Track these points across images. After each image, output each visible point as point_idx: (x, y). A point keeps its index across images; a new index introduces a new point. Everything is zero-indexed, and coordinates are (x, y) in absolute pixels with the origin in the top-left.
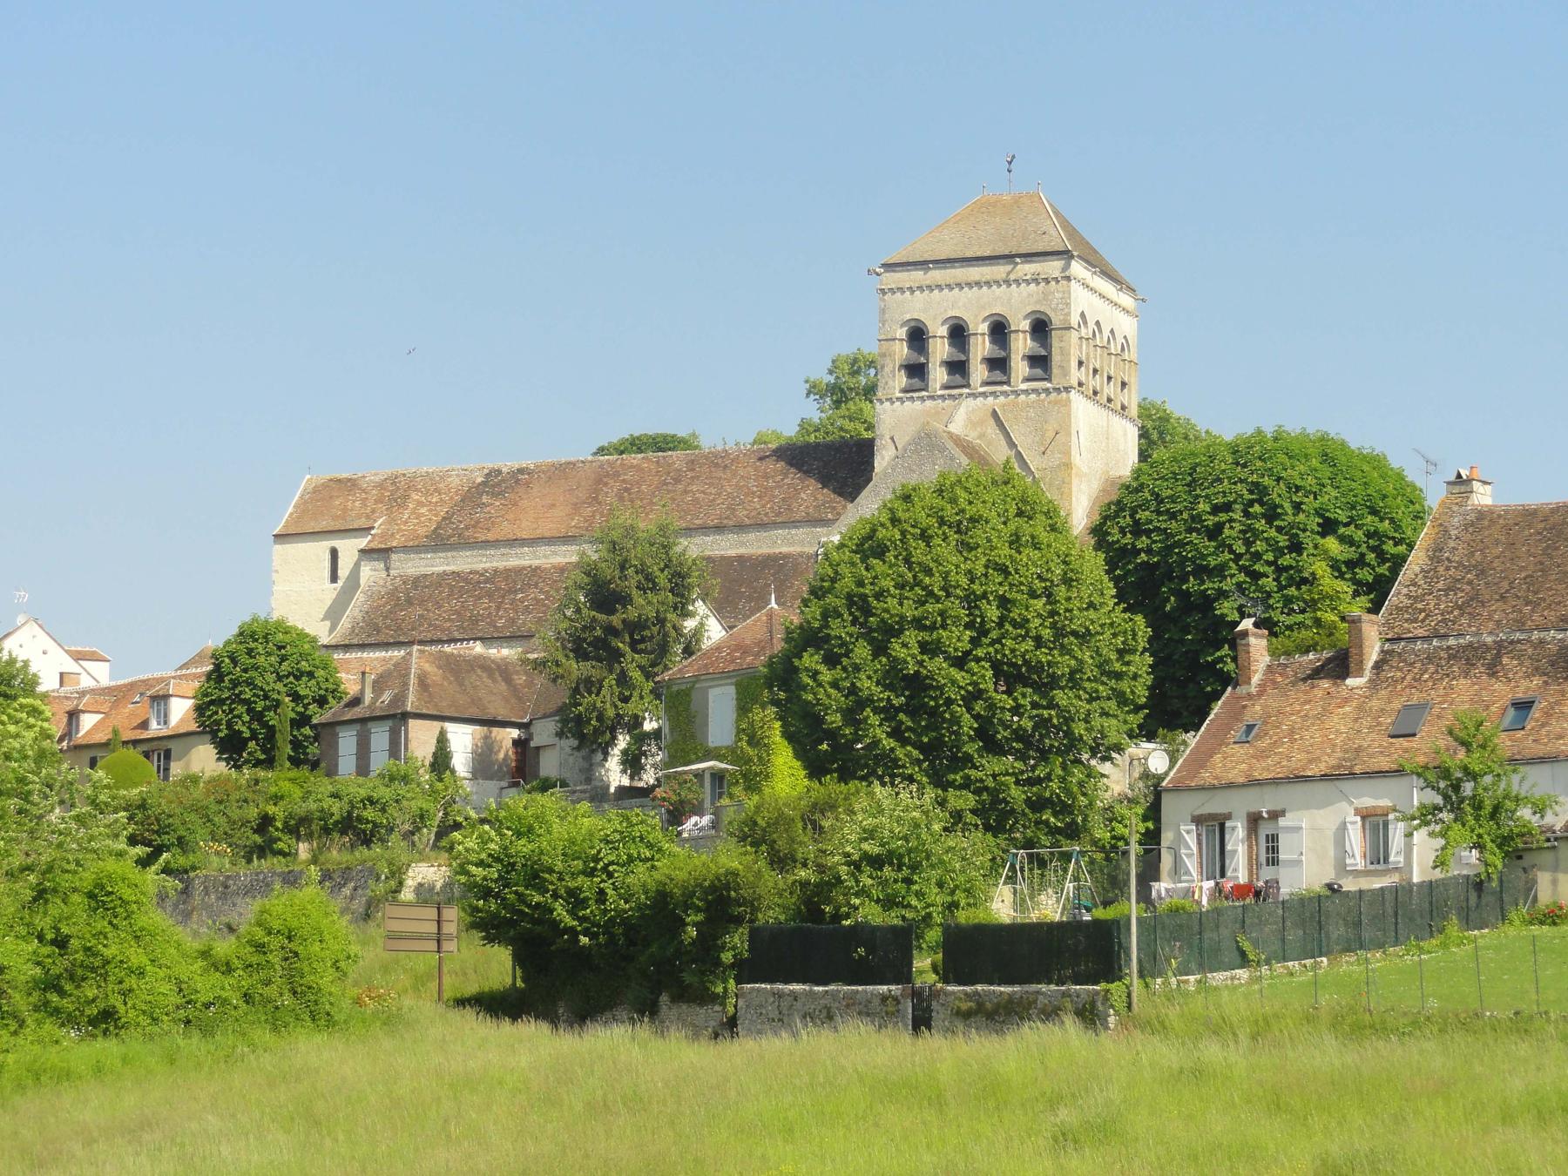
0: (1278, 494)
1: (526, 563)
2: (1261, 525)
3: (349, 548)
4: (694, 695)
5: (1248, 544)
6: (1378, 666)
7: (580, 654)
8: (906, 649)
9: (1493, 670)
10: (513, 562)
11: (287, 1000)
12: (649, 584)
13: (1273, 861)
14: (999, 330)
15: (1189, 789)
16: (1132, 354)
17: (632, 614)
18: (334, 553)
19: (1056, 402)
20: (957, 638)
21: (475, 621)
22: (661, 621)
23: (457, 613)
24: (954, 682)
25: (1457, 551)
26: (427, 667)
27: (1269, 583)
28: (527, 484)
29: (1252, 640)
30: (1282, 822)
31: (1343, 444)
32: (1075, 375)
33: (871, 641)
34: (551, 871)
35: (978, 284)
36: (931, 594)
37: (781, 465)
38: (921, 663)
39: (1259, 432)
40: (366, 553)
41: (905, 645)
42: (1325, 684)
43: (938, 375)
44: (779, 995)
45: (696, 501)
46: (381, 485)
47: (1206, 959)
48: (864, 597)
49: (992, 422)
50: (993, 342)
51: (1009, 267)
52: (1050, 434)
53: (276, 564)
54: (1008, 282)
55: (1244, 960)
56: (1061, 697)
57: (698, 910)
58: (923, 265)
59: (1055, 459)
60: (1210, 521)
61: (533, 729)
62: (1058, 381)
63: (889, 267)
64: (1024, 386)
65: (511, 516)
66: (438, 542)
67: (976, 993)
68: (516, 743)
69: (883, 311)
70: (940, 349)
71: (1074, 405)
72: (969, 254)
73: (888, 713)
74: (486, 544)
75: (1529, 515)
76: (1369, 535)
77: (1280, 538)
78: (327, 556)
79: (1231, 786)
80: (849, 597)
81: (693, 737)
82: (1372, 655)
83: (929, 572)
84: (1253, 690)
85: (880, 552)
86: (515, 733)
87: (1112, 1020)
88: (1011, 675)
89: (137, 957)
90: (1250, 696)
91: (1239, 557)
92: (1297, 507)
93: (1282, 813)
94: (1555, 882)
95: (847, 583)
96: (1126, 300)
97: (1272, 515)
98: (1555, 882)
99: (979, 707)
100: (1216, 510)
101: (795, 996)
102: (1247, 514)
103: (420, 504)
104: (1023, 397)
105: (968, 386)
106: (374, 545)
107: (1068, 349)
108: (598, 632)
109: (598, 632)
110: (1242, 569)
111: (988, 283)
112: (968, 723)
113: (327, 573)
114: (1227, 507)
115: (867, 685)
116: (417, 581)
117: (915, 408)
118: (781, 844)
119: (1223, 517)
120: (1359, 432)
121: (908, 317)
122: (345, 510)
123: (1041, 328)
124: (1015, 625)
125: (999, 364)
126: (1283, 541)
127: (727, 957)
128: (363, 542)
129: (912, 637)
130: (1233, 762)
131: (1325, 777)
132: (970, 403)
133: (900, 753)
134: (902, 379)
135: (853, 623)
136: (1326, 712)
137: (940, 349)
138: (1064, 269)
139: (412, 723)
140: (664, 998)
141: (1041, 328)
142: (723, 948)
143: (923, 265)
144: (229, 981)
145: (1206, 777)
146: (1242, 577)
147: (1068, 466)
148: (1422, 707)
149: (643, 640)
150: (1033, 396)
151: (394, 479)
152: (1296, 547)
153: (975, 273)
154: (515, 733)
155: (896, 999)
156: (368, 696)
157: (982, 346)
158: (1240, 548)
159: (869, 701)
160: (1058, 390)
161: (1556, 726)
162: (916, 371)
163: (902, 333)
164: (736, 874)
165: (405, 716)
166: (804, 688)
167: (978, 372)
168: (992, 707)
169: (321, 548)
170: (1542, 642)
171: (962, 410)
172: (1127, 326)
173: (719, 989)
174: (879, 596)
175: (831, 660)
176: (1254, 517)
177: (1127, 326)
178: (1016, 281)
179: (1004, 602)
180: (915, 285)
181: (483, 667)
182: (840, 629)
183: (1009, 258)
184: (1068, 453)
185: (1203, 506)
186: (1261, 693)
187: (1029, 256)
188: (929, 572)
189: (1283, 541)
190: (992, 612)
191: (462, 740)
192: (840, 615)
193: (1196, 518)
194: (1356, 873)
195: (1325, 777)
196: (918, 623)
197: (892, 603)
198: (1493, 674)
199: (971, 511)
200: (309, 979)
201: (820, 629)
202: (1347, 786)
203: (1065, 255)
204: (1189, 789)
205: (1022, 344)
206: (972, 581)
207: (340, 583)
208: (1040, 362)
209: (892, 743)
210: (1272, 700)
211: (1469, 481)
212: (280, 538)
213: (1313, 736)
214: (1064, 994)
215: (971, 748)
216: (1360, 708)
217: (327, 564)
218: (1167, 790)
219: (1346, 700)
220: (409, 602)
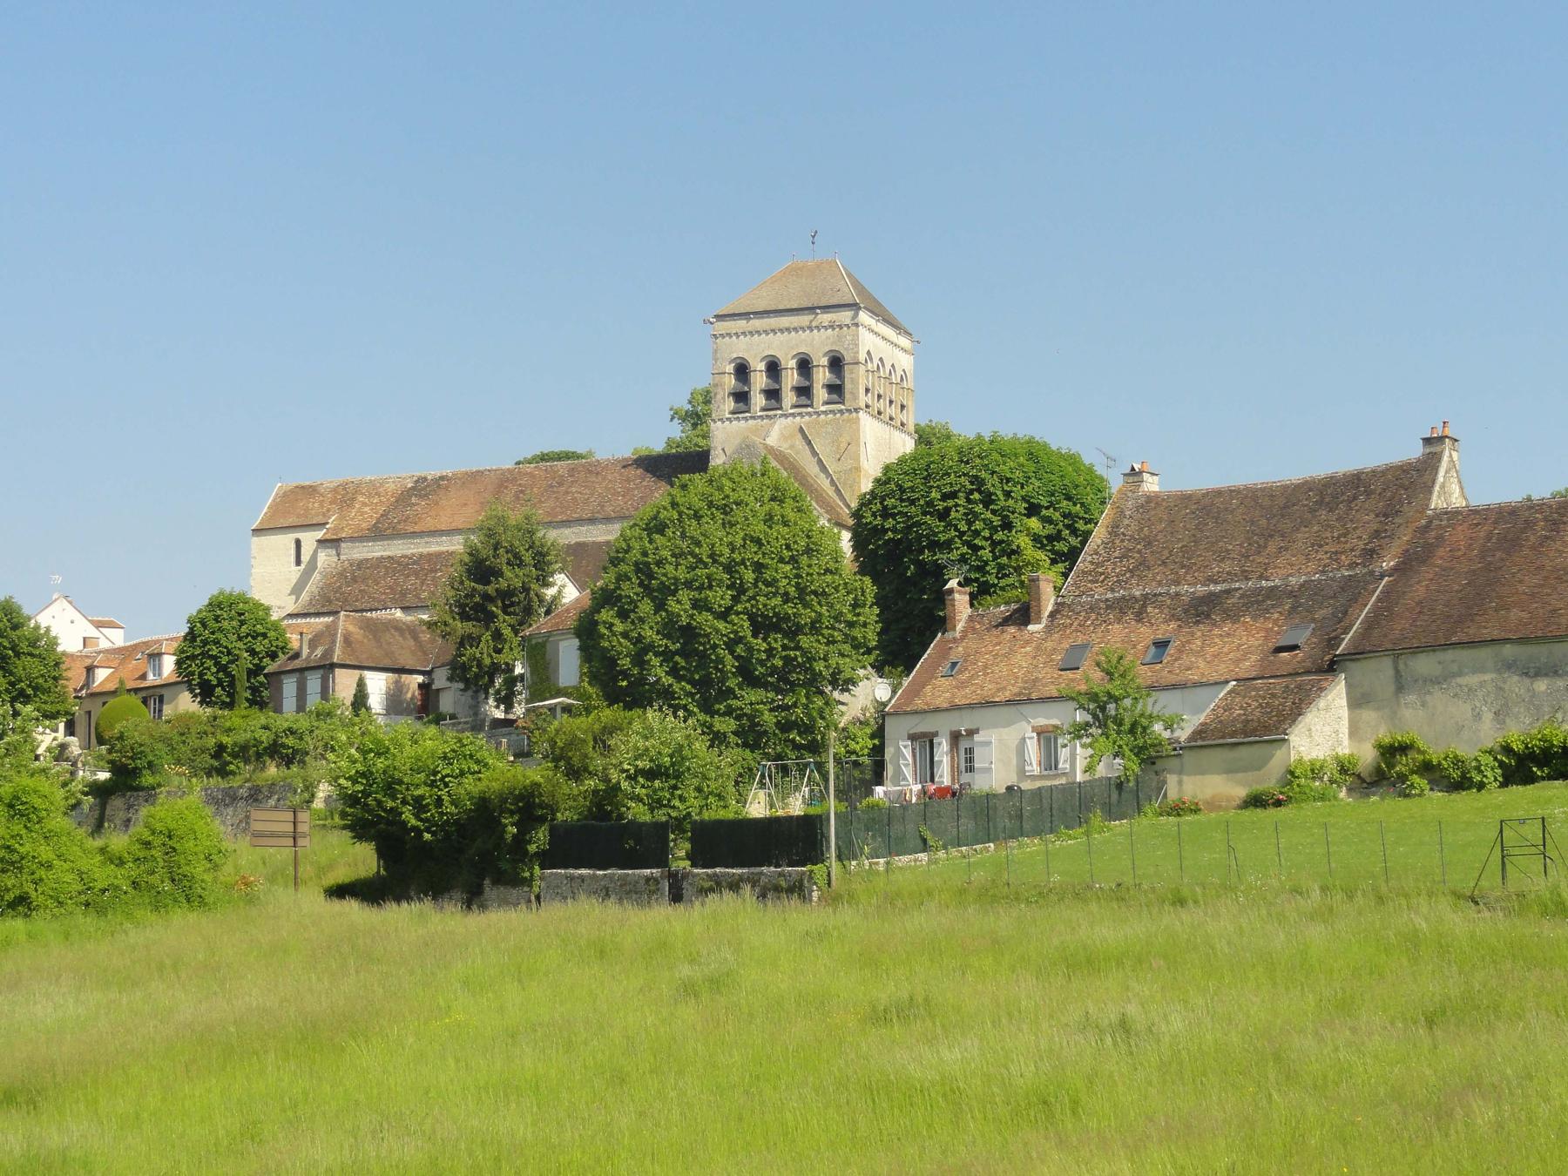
0: (992, 484)
1: (443, 549)
2: (979, 508)
3: (309, 539)
4: (548, 646)
5: (970, 523)
6: (1052, 615)
7: (464, 617)
8: (680, 605)
9: (1140, 617)
10: (434, 549)
11: (167, 886)
12: (516, 561)
13: (970, 769)
14: (805, 365)
15: (906, 713)
16: (911, 385)
17: (503, 584)
18: (298, 543)
20: (720, 597)
21: (403, 594)
22: (526, 589)
23: (391, 588)
24: (717, 631)
25: (1130, 526)
26: (351, 628)
27: (986, 554)
28: (447, 488)
29: (957, 596)
30: (977, 738)
31: (1045, 444)
32: (863, 399)
33: (653, 599)
34: (400, 782)
35: (788, 330)
36: (701, 561)
37: (639, 471)
38: (692, 616)
39: (979, 436)
40: (319, 541)
41: (679, 602)
42: (1012, 630)
43: (758, 400)
44: (572, 878)
45: (574, 499)
46: (335, 490)
47: (894, 846)
48: (647, 564)
49: (799, 436)
50: (800, 374)
52: (844, 445)
53: (254, 552)
54: (810, 328)
55: (925, 846)
56: (805, 641)
57: (512, 813)
58: (745, 315)
59: (847, 464)
60: (941, 506)
61: (434, 676)
62: (849, 404)
63: (720, 317)
64: (823, 408)
65: (433, 513)
66: (377, 533)
67: (715, 874)
68: (421, 686)
69: (716, 351)
70: (759, 380)
71: (862, 422)
72: (781, 307)
73: (667, 656)
74: (414, 535)
75: (1185, 499)
76: (1065, 516)
77: (994, 518)
78: (293, 546)
79: (937, 710)
80: (636, 564)
81: (548, 678)
82: (1049, 607)
83: (698, 544)
84: (958, 635)
85: (661, 528)
86: (420, 679)
87: (815, 894)
88: (762, 625)
89: (45, 852)
90: (955, 640)
91: (962, 534)
92: (1008, 494)
93: (977, 731)
94: (1180, 783)
95: (635, 555)
96: (904, 342)
97: (988, 501)
98: (1180, 783)
99: (739, 650)
100: (945, 497)
101: (582, 878)
102: (969, 501)
103: (364, 504)
105: (780, 408)
106: (328, 536)
107: (858, 380)
108: (477, 599)
109: (477, 599)
110: (966, 543)
111: (795, 329)
112: (730, 663)
113: (293, 559)
114: (953, 495)
115: (649, 634)
116: (361, 564)
117: (739, 426)
118: (576, 761)
119: (950, 503)
120: (1058, 437)
122: (307, 510)
123: (836, 363)
124: (768, 584)
125: (804, 391)
126: (997, 521)
127: (532, 848)
128: (320, 534)
129: (685, 595)
130: (940, 691)
131: (1009, 703)
133: (676, 687)
134: (730, 404)
135: (640, 585)
136: (1012, 651)
137: (759, 380)
139: (338, 671)
140: (487, 882)
141: (836, 363)
142: (529, 842)
143: (745, 315)
144: (121, 872)
145: (919, 703)
146: (965, 549)
147: (858, 469)
148: (1084, 647)
149: (512, 604)
151: (344, 486)
152: (1007, 526)
153: (785, 321)
154: (420, 679)
155: (656, 881)
156: (305, 651)
157: (791, 378)
158: (963, 527)
159: (650, 647)
160: (849, 411)
161: (1186, 660)
162: (742, 397)
163: (730, 368)
164: (538, 785)
165: (332, 666)
166: (602, 636)
167: (789, 398)
168: (750, 649)
169: (287, 540)
170: (1177, 594)
172: (905, 362)
173: (527, 874)
174: (659, 563)
175: (623, 615)
176: (975, 502)
177: (905, 362)
179: (759, 567)
181: (397, 628)
182: (630, 590)
183: (811, 310)
184: (857, 459)
185: (935, 494)
186: (963, 638)
187: (827, 308)
188: (698, 544)
189: (997, 521)
190: (749, 576)
191: (377, 685)
192: (629, 579)
193: (930, 504)
194: (1033, 778)
195: (1009, 703)
196: (688, 584)
197: (670, 568)
198: (1139, 621)
199: (734, 497)
200: (185, 869)
201: (614, 591)
202: (1027, 709)
203: (855, 307)
204: (906, 713)
205: (822, 376)
206: (733, 551)
207: (303, 566)
208: (836, 389)
209: (671, 680)
210: (971, 643)
211: (1141, 472)
212: (257, 532)
213: (1002, 669)
214: (780, 874)
215: (732, 683)
216: (1038, 648)
217: (293, 552)
218: (889, 714)
219: (1027, 642)
220: (354, 580)
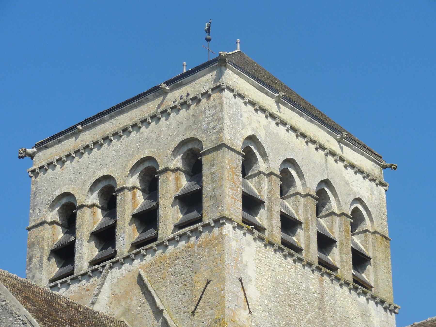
19: (207, 243)
35: (125, 130)
49: (137, 290)
51: (158, 101)
63: (42, 146)
104: (171, 248)
121: (58, 193)
132: (116, 274)
138: (217, 79)
143: (72, 131)
150: (182, 244)
163: (54, 215)
171: (107, 285)
178: (164, 112)
180: (63, 155)
187: (176, 82)
205: (173, 185)
